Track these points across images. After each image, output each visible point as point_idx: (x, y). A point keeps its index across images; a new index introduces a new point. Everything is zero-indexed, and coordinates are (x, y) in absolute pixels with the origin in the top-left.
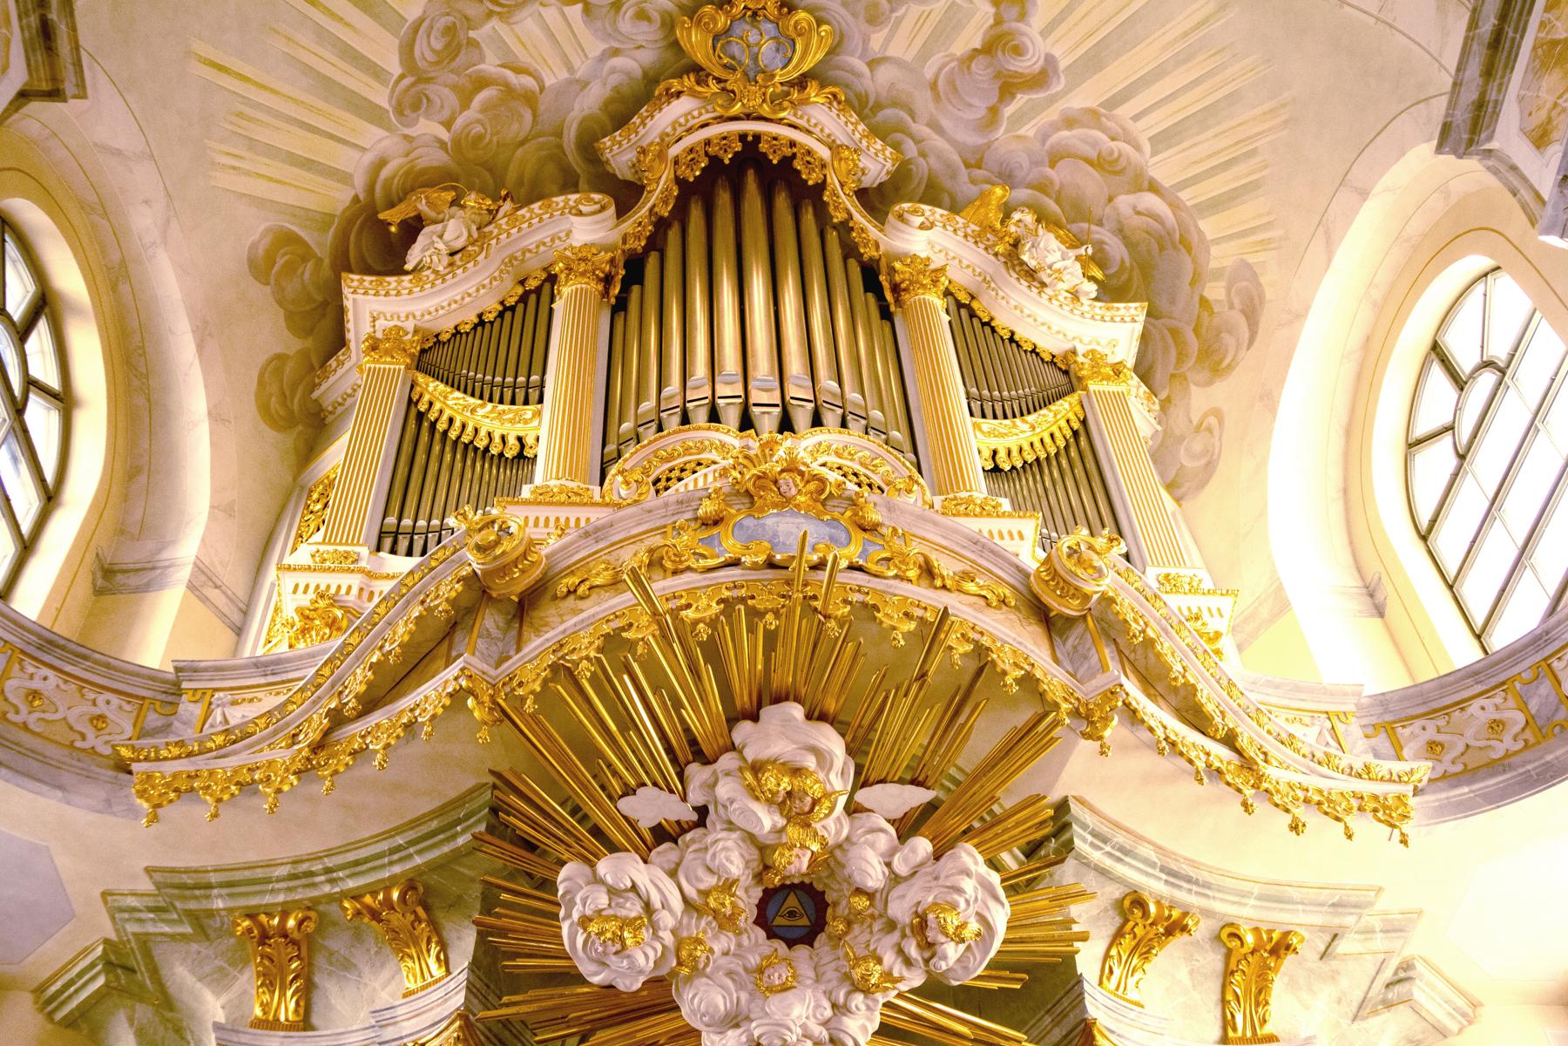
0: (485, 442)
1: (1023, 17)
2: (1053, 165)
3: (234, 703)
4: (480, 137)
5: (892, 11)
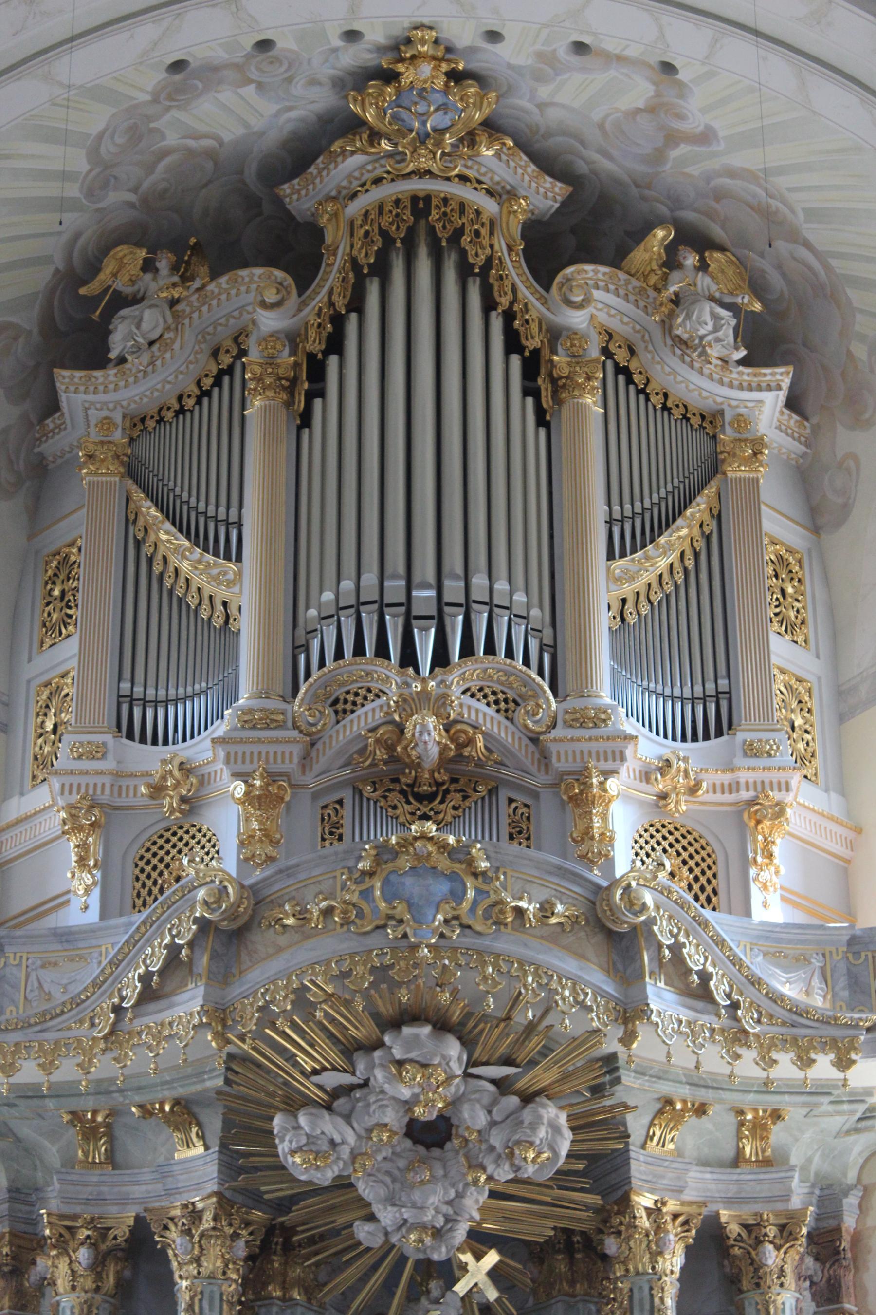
0: (197, 602)
1: (682, 96)
2: (718, 199)
3: (43, 966)
4: (165, 191)
5: (557, 75)
